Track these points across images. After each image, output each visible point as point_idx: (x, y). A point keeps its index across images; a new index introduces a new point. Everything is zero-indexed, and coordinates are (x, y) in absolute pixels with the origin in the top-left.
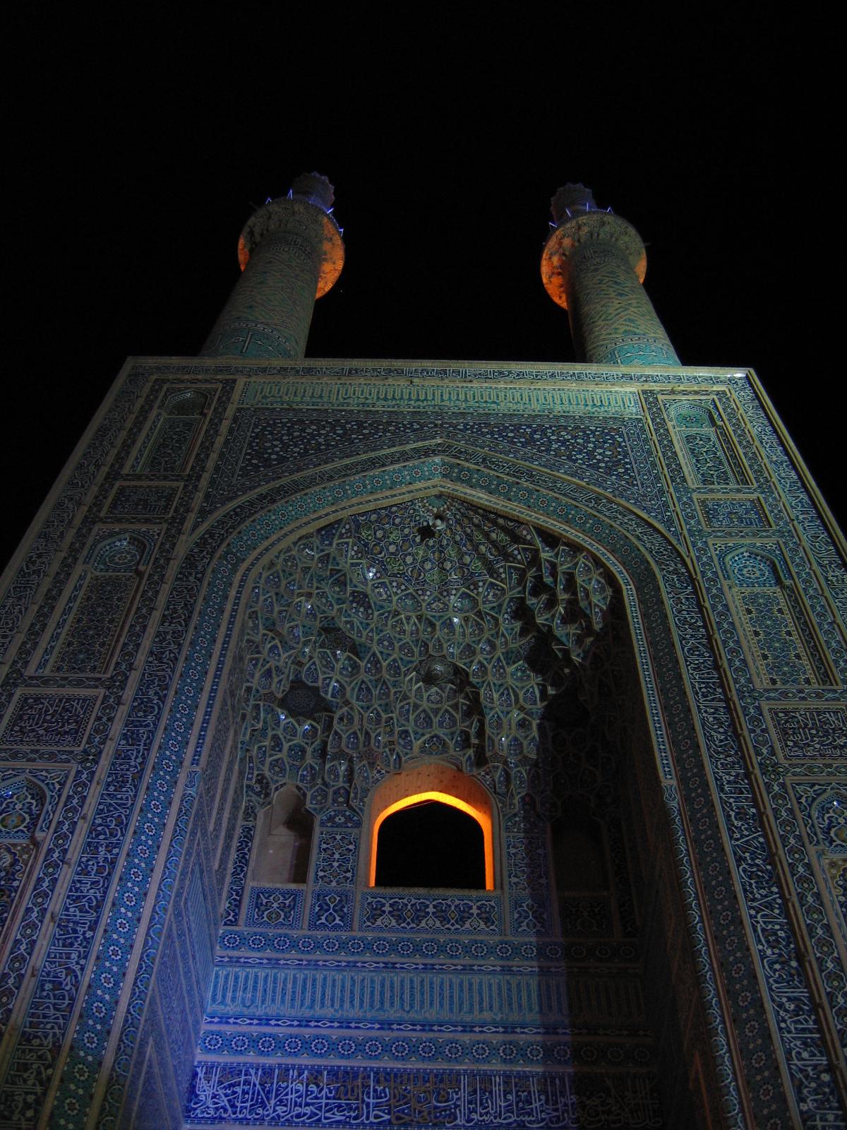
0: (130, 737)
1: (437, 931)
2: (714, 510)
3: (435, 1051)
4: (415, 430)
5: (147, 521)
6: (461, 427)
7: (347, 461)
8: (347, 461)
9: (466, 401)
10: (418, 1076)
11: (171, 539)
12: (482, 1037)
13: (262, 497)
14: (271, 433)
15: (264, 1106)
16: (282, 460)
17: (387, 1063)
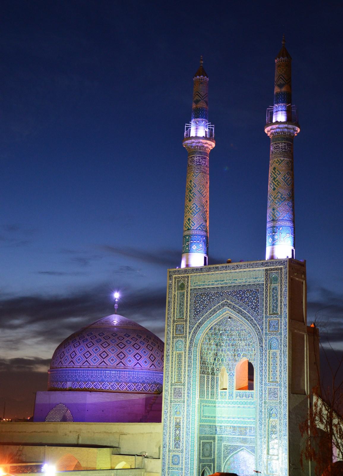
0: (188, 396)
1: (245, 400)
2: (271, 324)
3: (245, 423)
4: (222, 296)
5: (181, 337)
6: (229, 293)
7: (210, 311)
8: (210, 311)
9: (231, 280)
10: (242, 427)
11: (186, 342)
12: (251, 420)
13: (198, 326)
14: (197, 300)
15: (225, 432)
16: (200, 311)
17: (239, 425)
